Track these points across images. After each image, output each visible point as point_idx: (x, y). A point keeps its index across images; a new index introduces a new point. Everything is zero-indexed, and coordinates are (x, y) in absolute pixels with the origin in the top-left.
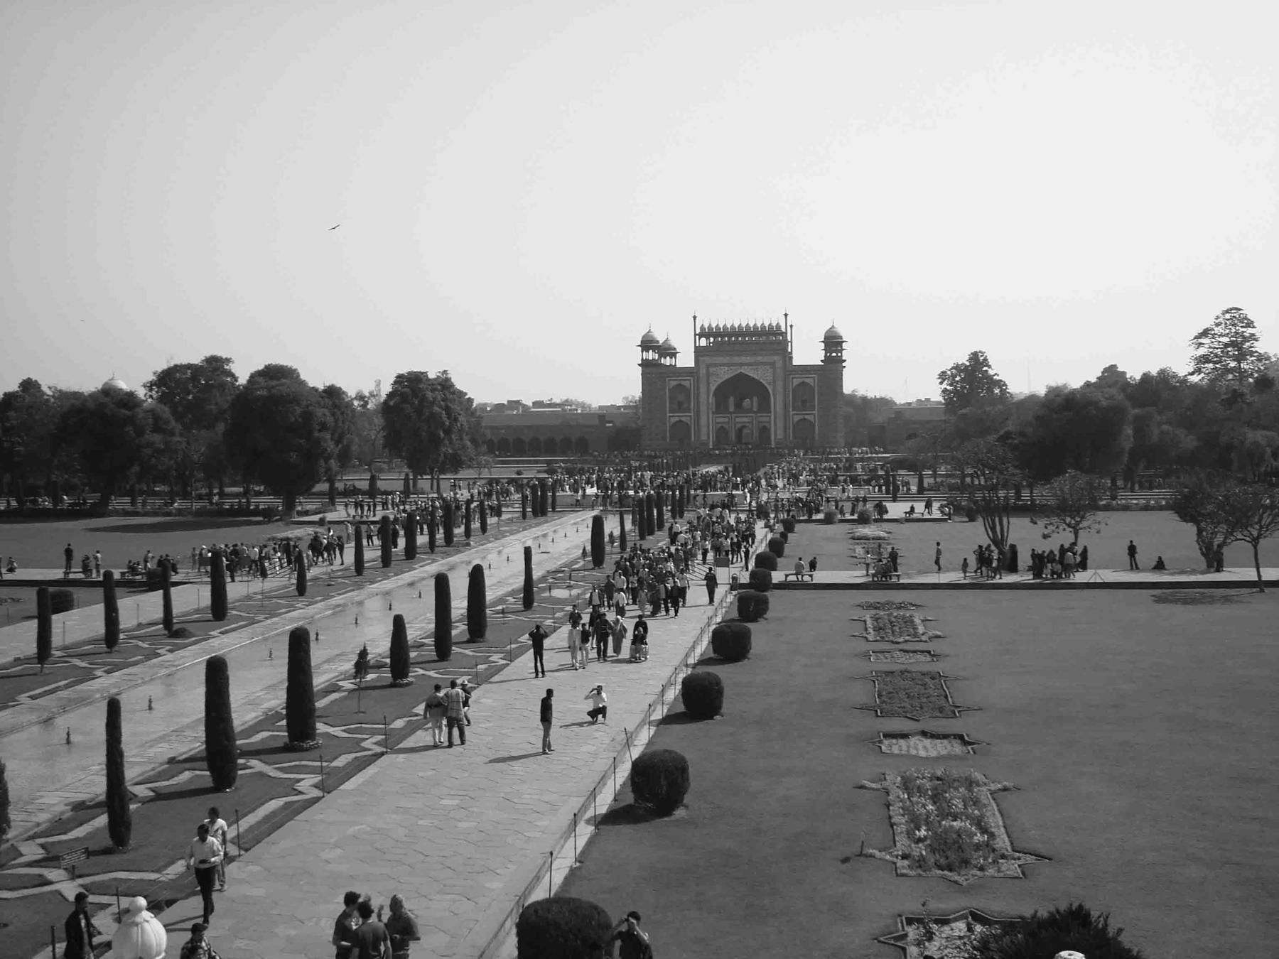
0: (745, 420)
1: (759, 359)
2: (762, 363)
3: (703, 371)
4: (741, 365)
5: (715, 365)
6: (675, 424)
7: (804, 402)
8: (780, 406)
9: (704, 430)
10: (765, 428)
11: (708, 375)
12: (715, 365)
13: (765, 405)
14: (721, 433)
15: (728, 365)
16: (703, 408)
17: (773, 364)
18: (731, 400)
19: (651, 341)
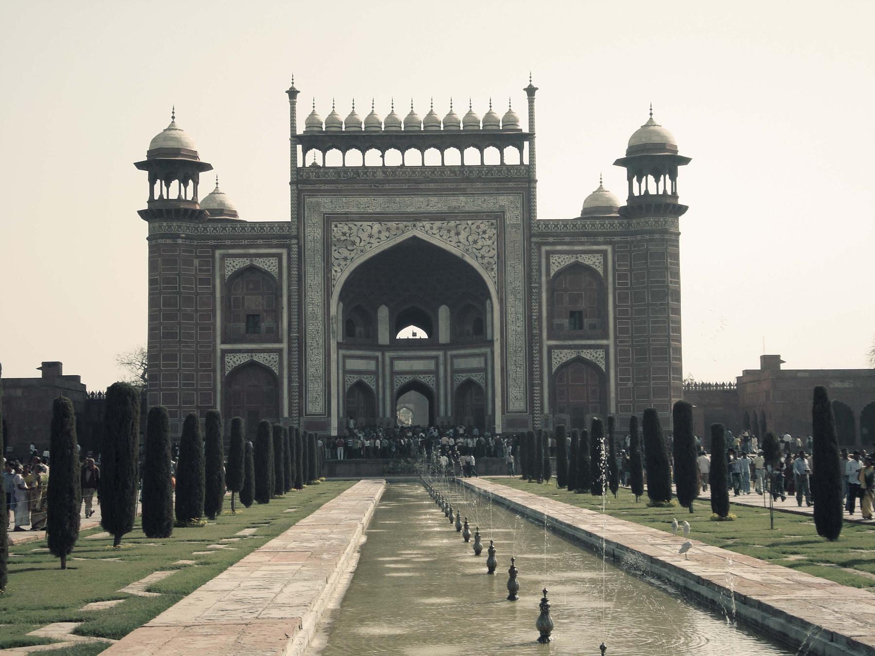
0: (419, 365)
1: (462, 202)
2: (475, 215)
3: (313, 233)
4: (416, 217)
5: (347, 218)
6: (239, 370)
7: (576, 317)
8: (516, 328)
9: (315, 389)
10: (469, 383)
11: (327, 244)
12: (347, 218)
13: (472, 327)
14: (360, 396)
15: (380, 217)
16: (314, 327)
17: (497, 217)
18: (383, 313)
19: (177, 151)
